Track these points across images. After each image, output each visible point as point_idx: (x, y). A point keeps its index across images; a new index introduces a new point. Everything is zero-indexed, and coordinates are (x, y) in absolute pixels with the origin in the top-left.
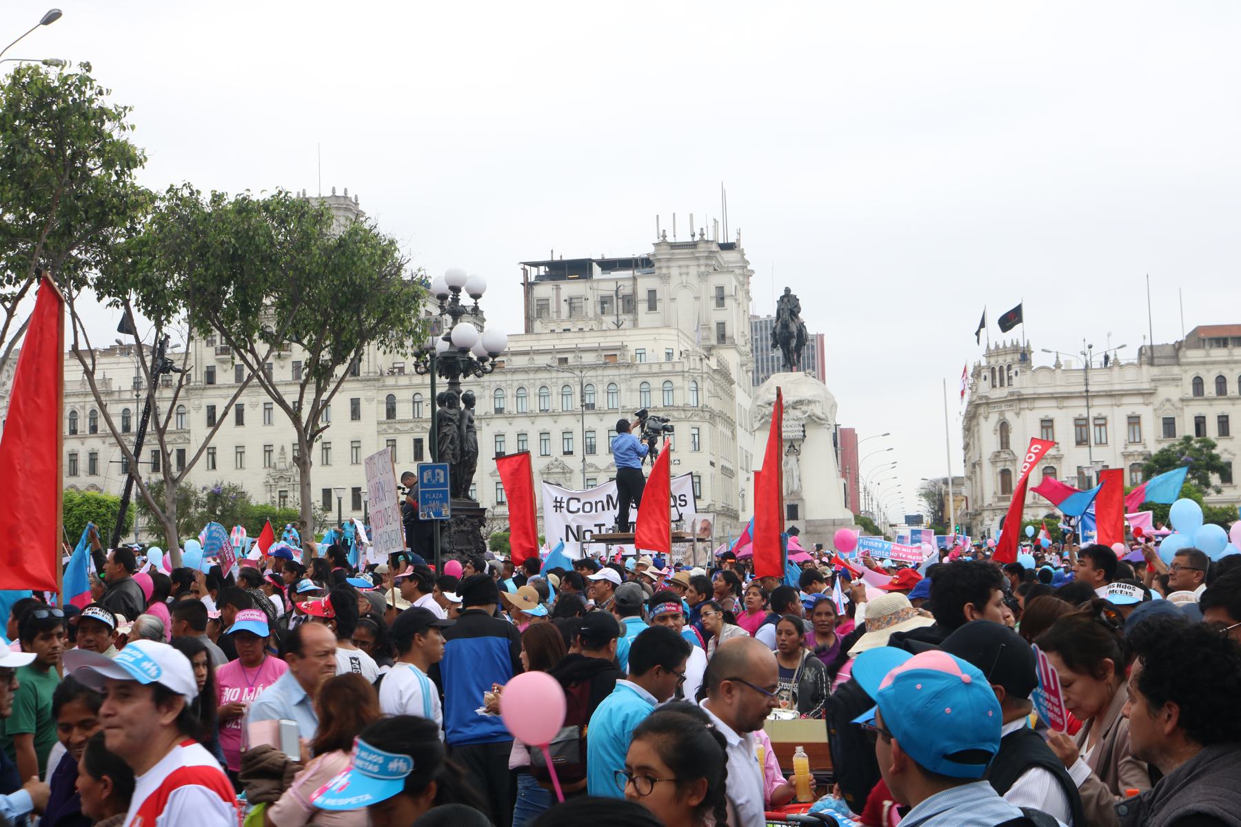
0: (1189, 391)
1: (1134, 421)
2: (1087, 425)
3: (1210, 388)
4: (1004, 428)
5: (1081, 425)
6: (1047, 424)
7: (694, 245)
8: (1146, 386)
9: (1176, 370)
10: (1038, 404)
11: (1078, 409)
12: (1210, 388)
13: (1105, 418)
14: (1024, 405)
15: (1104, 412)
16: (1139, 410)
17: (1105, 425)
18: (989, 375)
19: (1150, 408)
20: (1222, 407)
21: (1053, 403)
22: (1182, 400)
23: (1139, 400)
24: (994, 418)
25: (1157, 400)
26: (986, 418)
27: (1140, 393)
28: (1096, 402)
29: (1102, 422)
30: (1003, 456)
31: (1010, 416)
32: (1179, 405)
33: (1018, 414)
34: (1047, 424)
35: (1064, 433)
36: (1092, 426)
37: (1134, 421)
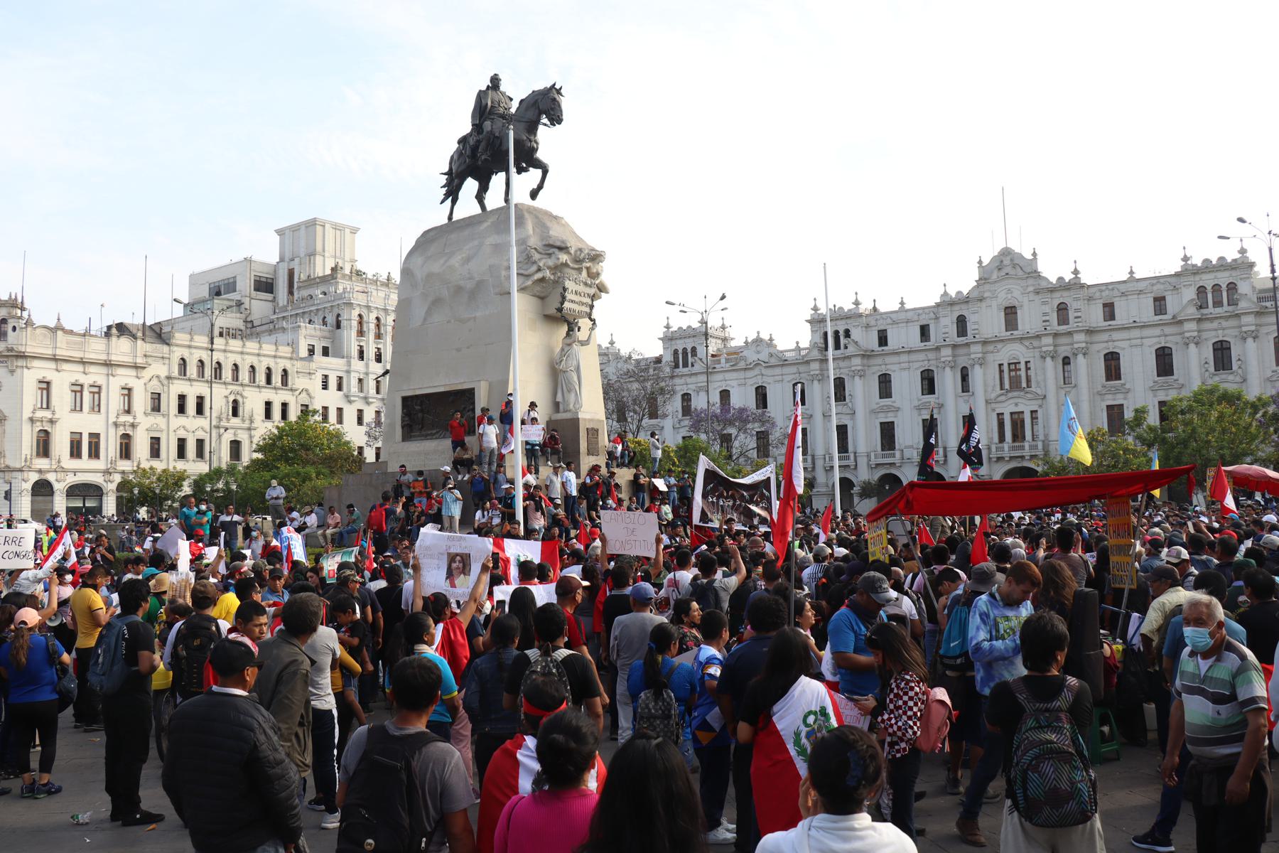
0: (176, 373)
1: (128, 392)
2: (81, 392)
3: (192, 370)
5: (78, 389)
8: (140, 361)
9: (166, 348)
10: (36, 363)
11: (72, 374)
12: (192, 370)
13: (99, 387)
14: (21, 362)
15: (101, 380)
16: (132, 382)
17: (99, 393)
19: (142, 381)
20: (201, 389)
21: (52, 365)
22: (169, 378)
23: (133, 372)
25: (147, 374)
27: (136, 367)
28: (92, 369)
29: (97, 390)
32: (165, 382)
33: (12, 372)
34: (46, 386)
35: (62, 397)
36: (86, 393)
37: (128, 392)
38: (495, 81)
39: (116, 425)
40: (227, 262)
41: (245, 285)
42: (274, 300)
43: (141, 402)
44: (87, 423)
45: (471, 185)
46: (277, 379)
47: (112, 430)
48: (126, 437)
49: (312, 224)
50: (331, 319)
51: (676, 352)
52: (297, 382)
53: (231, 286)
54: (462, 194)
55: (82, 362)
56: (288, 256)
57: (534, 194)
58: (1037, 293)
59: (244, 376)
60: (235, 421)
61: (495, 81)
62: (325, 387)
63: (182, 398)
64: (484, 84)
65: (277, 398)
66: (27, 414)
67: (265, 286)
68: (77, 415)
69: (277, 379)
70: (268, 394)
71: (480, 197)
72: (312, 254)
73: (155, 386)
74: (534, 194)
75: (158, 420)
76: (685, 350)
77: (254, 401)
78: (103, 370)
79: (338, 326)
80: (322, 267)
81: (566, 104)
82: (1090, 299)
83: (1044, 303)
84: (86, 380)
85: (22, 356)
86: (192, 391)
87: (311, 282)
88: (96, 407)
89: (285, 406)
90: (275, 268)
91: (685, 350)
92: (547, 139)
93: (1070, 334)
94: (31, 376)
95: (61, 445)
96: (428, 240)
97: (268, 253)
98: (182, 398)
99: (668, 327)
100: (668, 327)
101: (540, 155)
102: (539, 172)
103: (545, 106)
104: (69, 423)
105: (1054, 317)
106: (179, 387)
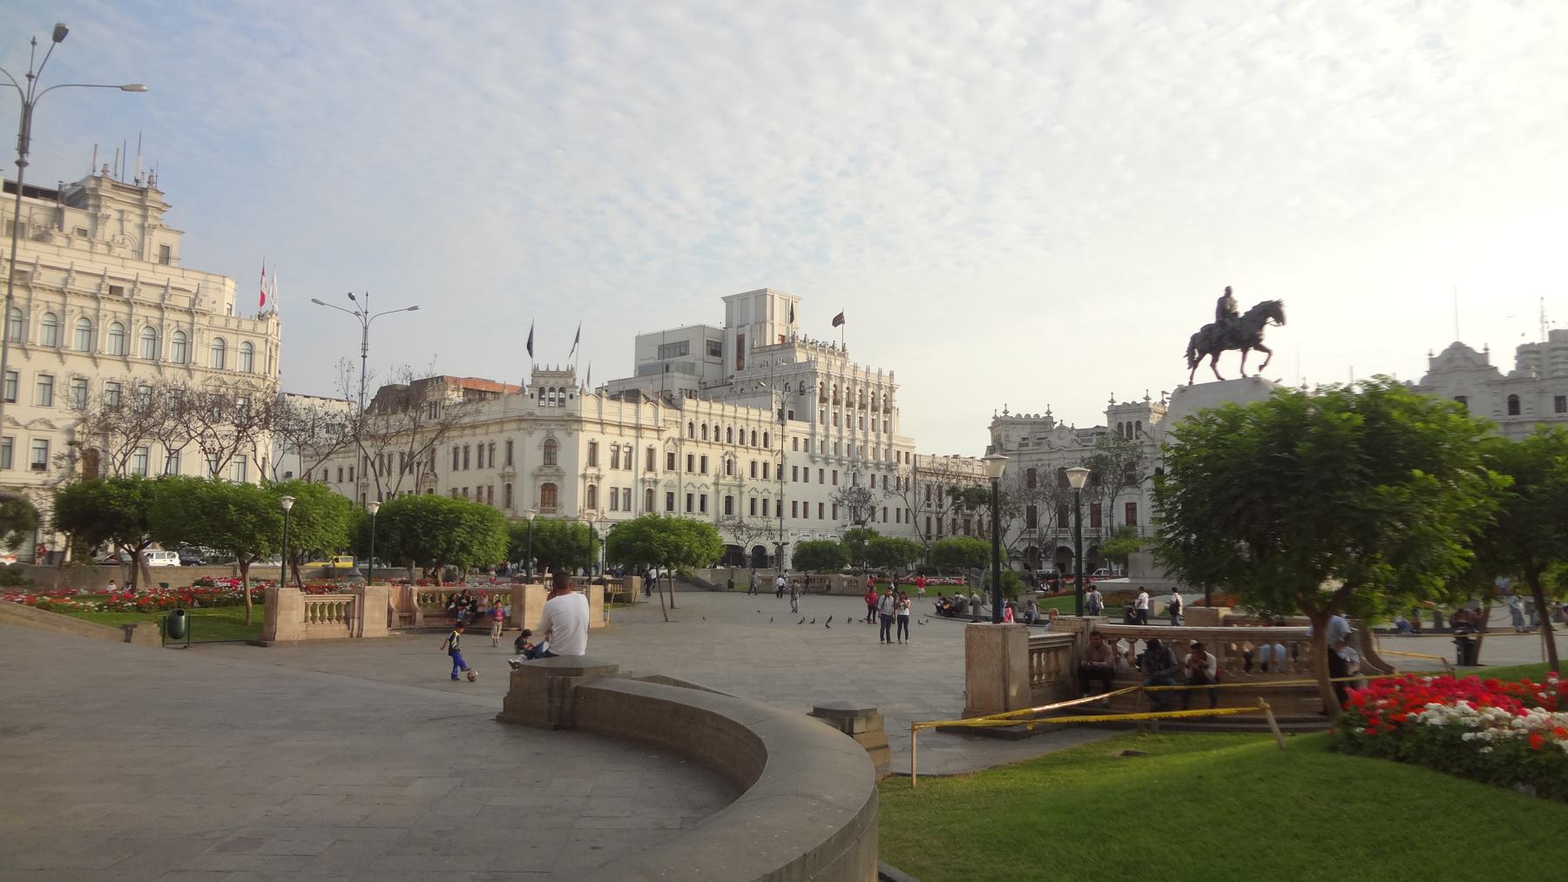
0: (686, 436)
4: (550, 448)
6: (593, 446)
7: (142, 192)
8: (661, 424)
10: (588, 427)
14: (575, 426)
15: (632, 443)
18: (536, 394)
22: (681, 440)
24: (539, 436)
25: (665, 436)
26: (530, 434)
27: (658, 430)
28: (627, 431)
30: (546, 471)
31: (559, 435)
33: (570, 434)
34: (593, 446)
35: (604, 456)
38: (1228, 291)
39: (643, 481)
40: (678, 326)
41: (698, 350)
42: (722, 363)
43: (660, 461)
44: (624, 479)
45: (1208, 357)
46: (760, 440)
47: (640, 485)
48: (650, 491)
49: (761, 295)
50: (794, 386)
51: (1120, 425)
52: (776, 444)
53: (681, 347)
54: (1201, 364)
55: (620, 426)
56: (736, 322)
57: (1261, 367)
58: (1489, 384)
59: (736, 437)
60: (729, 478)
61: (1228, 291)
62: (795, 449)
63: (690, 457)
64: (1222, 294)
65: (761, 458)
66: (581, 471)
67: (716, 350)
68: (615, 472)
69: (760, 440)
70: (754, 455)
71: (1213, 365)
72: (761, 323)
73: (671, 448)
74: (1261, 367)
75: (672, 476)
76: (1129, 424)
77: (743, 461)
78: (633, 432)
79: (802, 392)
80: (773, 337)
81: (1287, 310)
82: (1542, 392)
83: (1496, 394)
84: (621, 441)
85: (579, 421)
86: (698, 452)
87: (764, 349)
88: (628, 467)
89: (765, 465)
90: (724, 332)
91: (1129, 424)
92: (1270, 333)
93: (1521, 423)
94: (584, 438)
95: (604, 500)
96: (1182, 391)
97: (715, 318)
98: (690, 457)
99: (1112, 401)
100: (1112, 401)
101: (1264, 343)
102: (1263, 356)
103: (1271, 311)
104: (611, 479)
105: (1505, 408)
106: (688, 448)
